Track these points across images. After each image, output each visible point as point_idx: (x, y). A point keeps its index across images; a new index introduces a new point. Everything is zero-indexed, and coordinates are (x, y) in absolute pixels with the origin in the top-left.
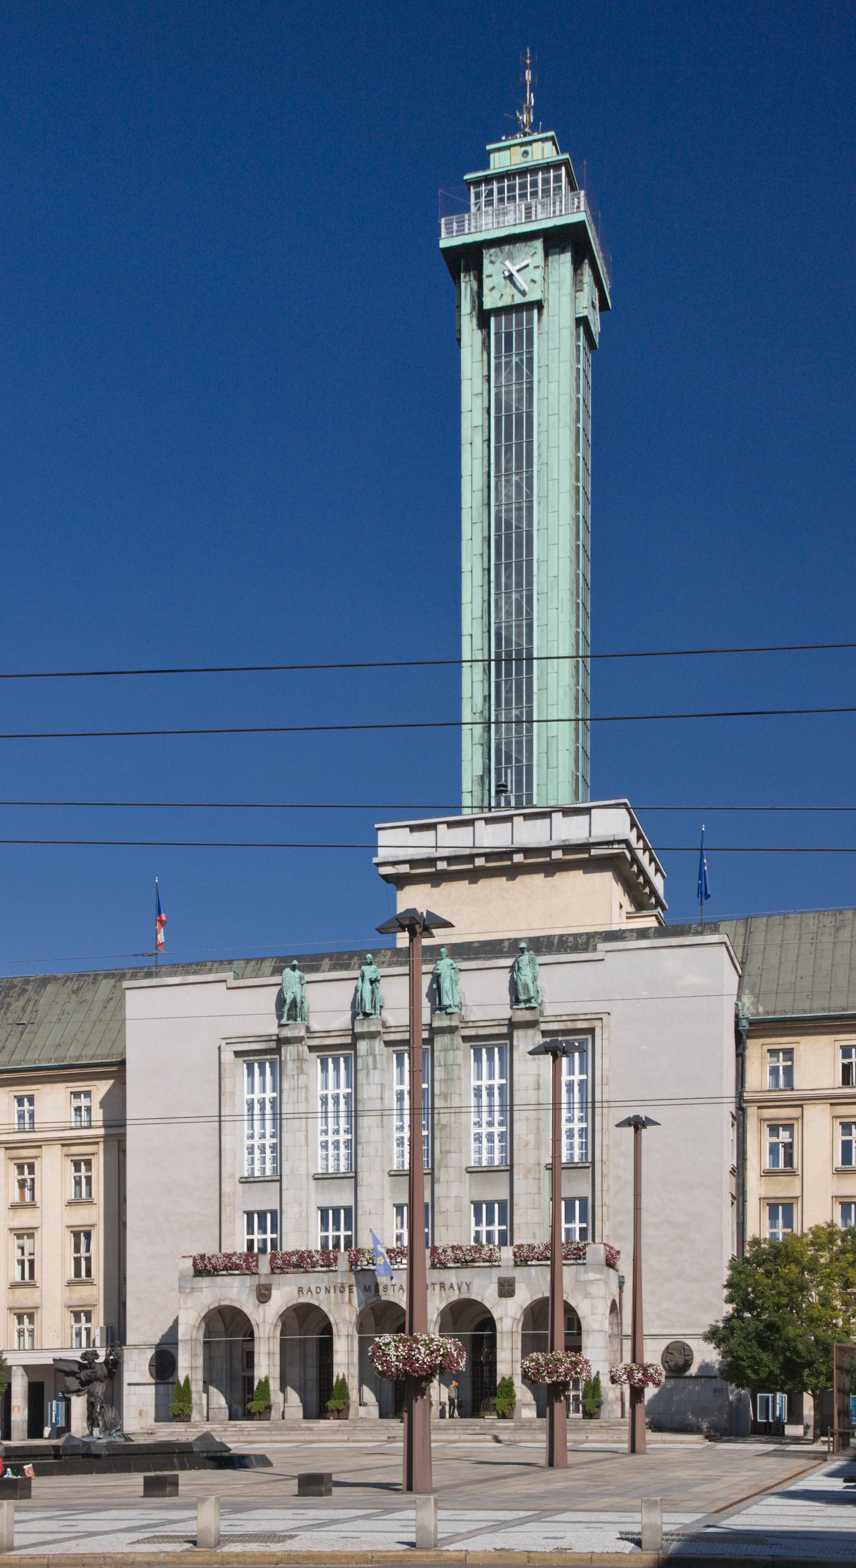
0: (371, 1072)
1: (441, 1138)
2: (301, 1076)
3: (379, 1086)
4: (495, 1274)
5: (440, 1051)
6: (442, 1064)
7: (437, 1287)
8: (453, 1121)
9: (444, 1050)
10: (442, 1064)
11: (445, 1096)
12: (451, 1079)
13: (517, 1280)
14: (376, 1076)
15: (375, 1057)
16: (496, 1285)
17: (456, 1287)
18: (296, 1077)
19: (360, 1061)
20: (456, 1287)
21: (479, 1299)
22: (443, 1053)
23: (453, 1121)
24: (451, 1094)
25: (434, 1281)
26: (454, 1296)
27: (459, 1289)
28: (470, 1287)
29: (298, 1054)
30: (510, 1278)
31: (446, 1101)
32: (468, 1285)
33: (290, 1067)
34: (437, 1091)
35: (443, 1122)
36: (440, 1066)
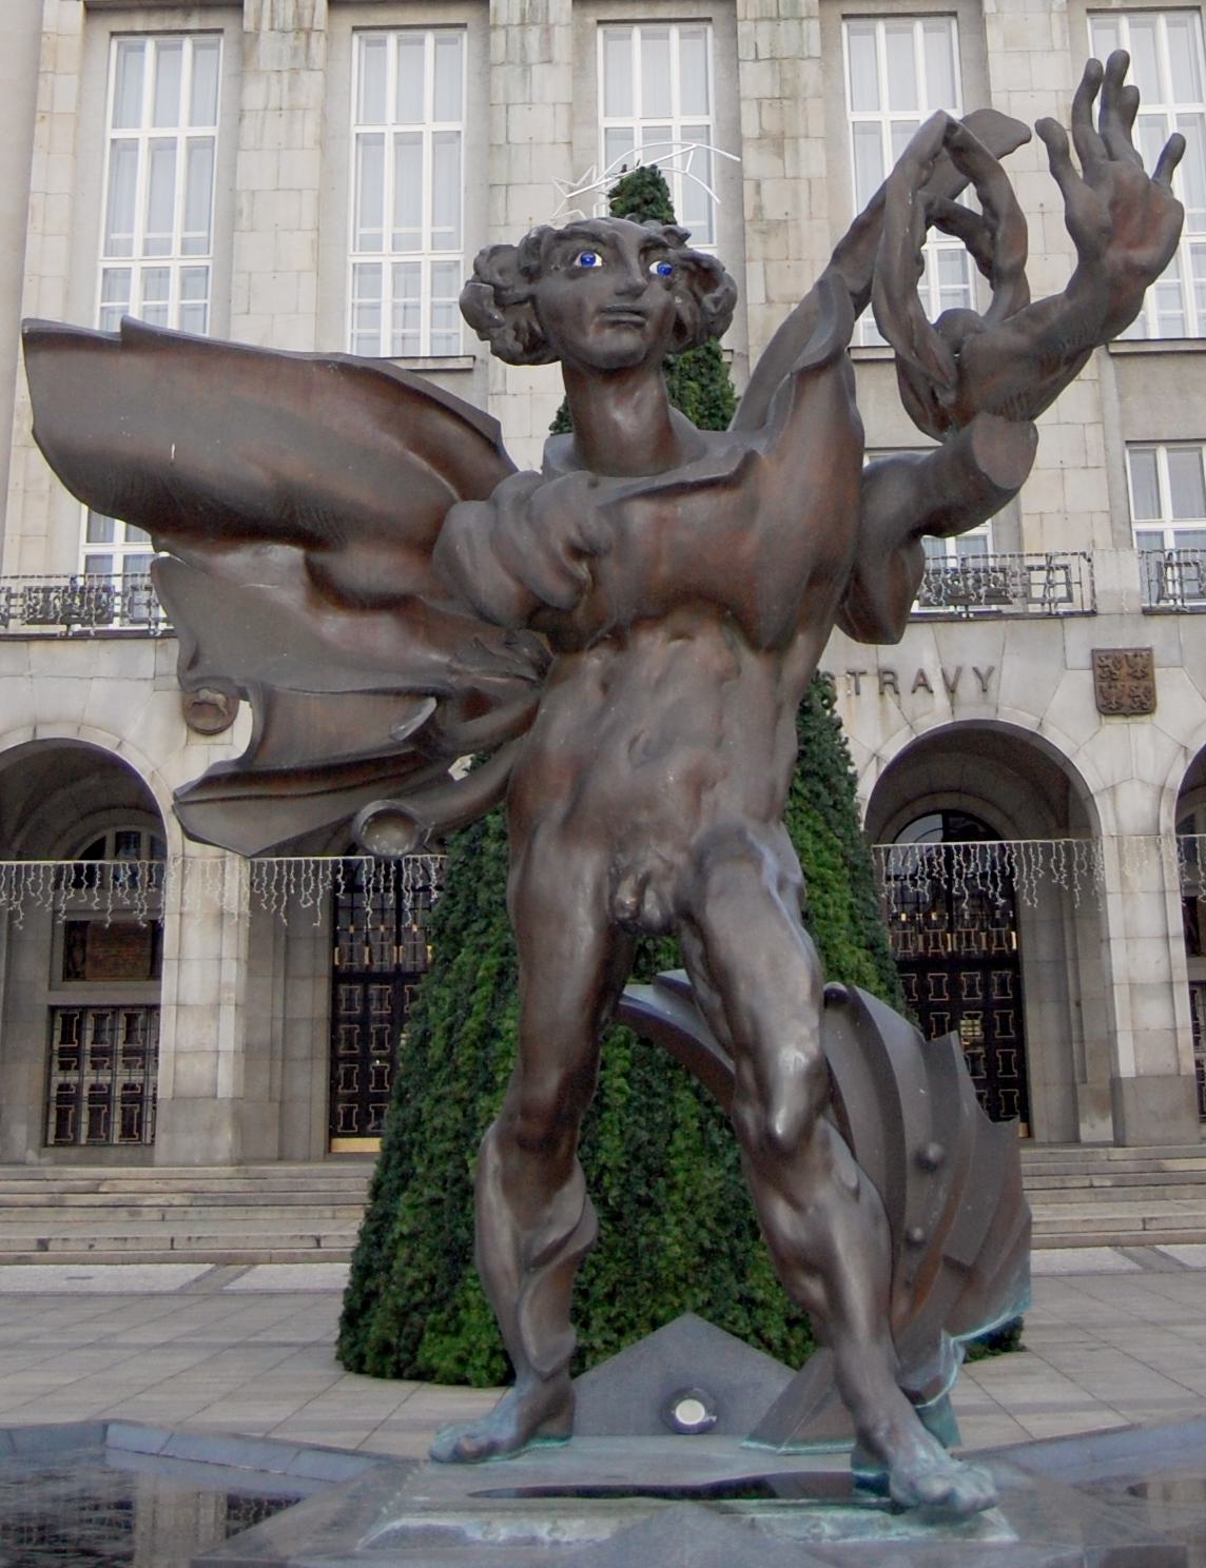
0: (537, 70)
1: (766, 260)
2: (304, 75)
3: (563, 112)
4: (1080, 641)
5: (756, 20)
6: (764, 53)
7: (869, 685)
8: (805, 211)
9: (771, 19)
10: (764, 53)
11: (777, 143)
12: (794, 97)
13: (1156, 660)
14: (551, 83)
15: (547, 30)
16: (1086, 679)
17: (937, 684)
18: (286, 76)
19: (498, 38)
20: (937, 684)
21: (1025, 721)
22: (765, 27)
23: (805, 211)
24: (795, 138)
25: (858, 665)
26: (935, 714)
27: (951, 690)
28: (992, 685)
29: (298, 17)
30: (1137, 653)
31: (780, 155)
32: (984, 678)
33: (270, 49)
34: (749, 128)
35: (773, 213)
36: (757, 59)
